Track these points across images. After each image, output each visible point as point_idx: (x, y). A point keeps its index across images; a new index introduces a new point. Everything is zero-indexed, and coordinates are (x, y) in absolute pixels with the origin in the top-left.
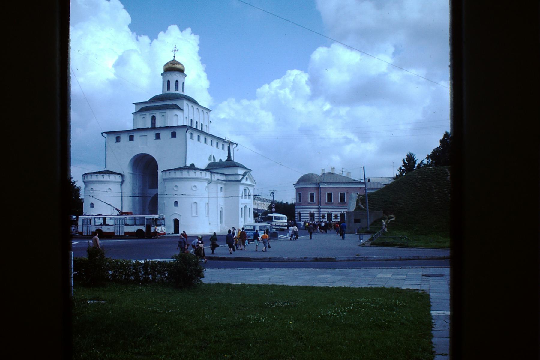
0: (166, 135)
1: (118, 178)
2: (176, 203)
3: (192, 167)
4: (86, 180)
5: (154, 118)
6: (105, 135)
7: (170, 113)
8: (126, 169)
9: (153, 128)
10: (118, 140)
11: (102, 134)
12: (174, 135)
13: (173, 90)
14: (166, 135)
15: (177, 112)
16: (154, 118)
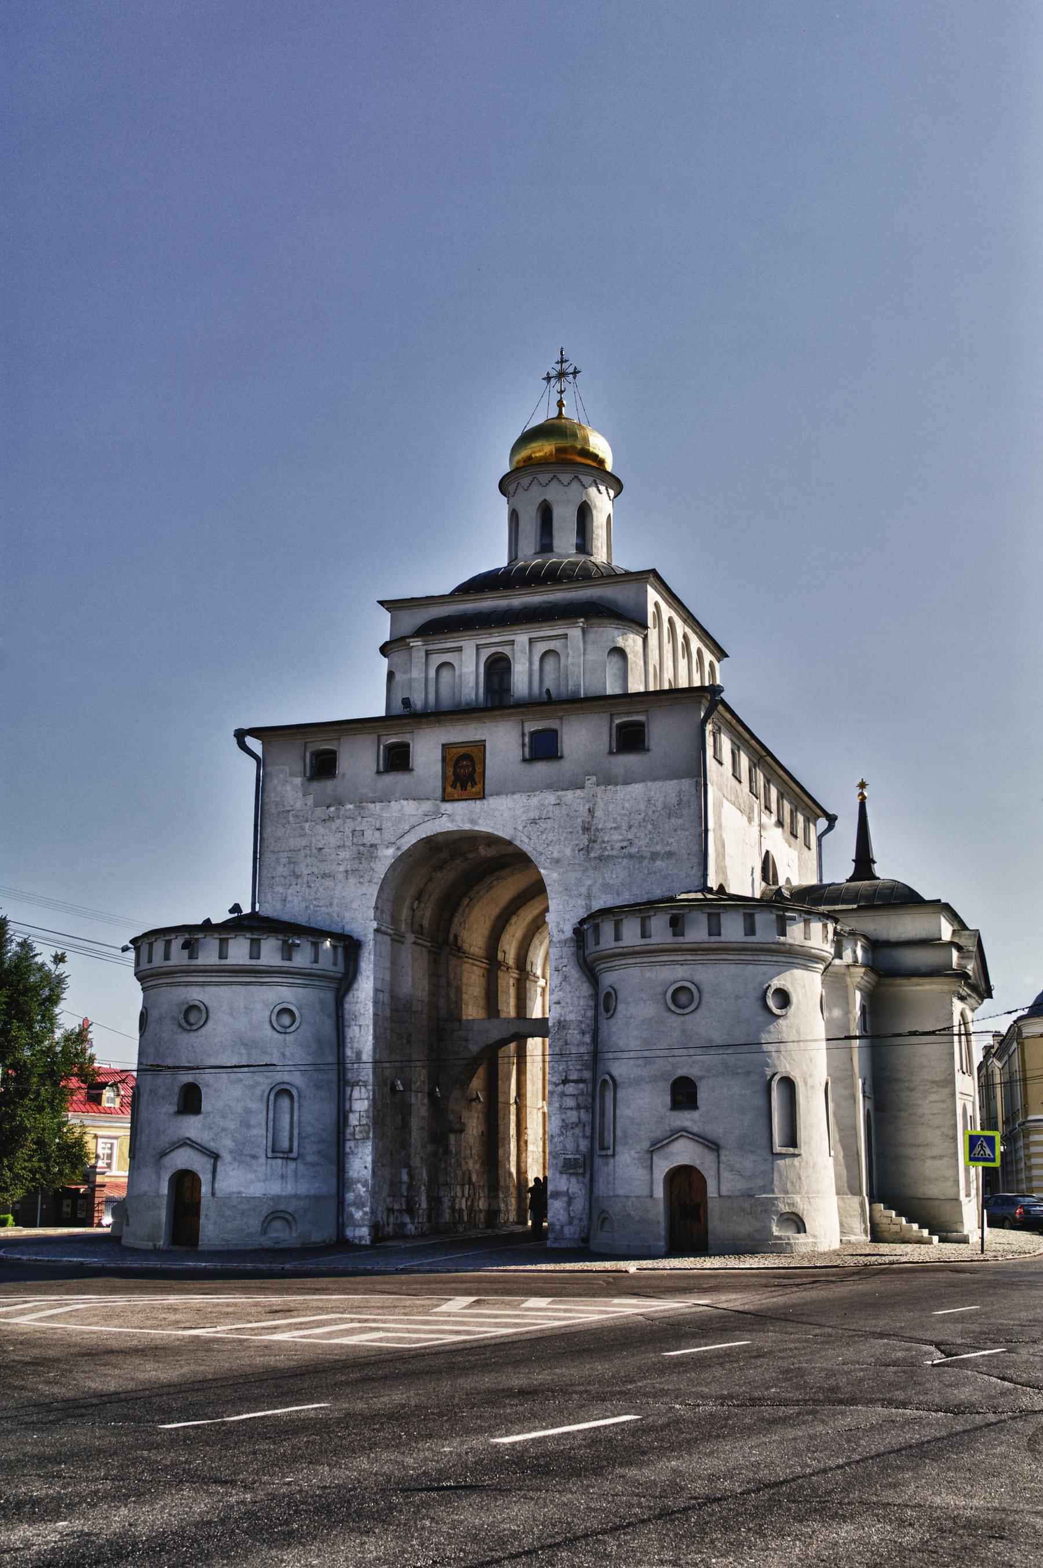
6: (255, 744)
10: (323, 766)
11: (240, 735)
16: (498, 669)
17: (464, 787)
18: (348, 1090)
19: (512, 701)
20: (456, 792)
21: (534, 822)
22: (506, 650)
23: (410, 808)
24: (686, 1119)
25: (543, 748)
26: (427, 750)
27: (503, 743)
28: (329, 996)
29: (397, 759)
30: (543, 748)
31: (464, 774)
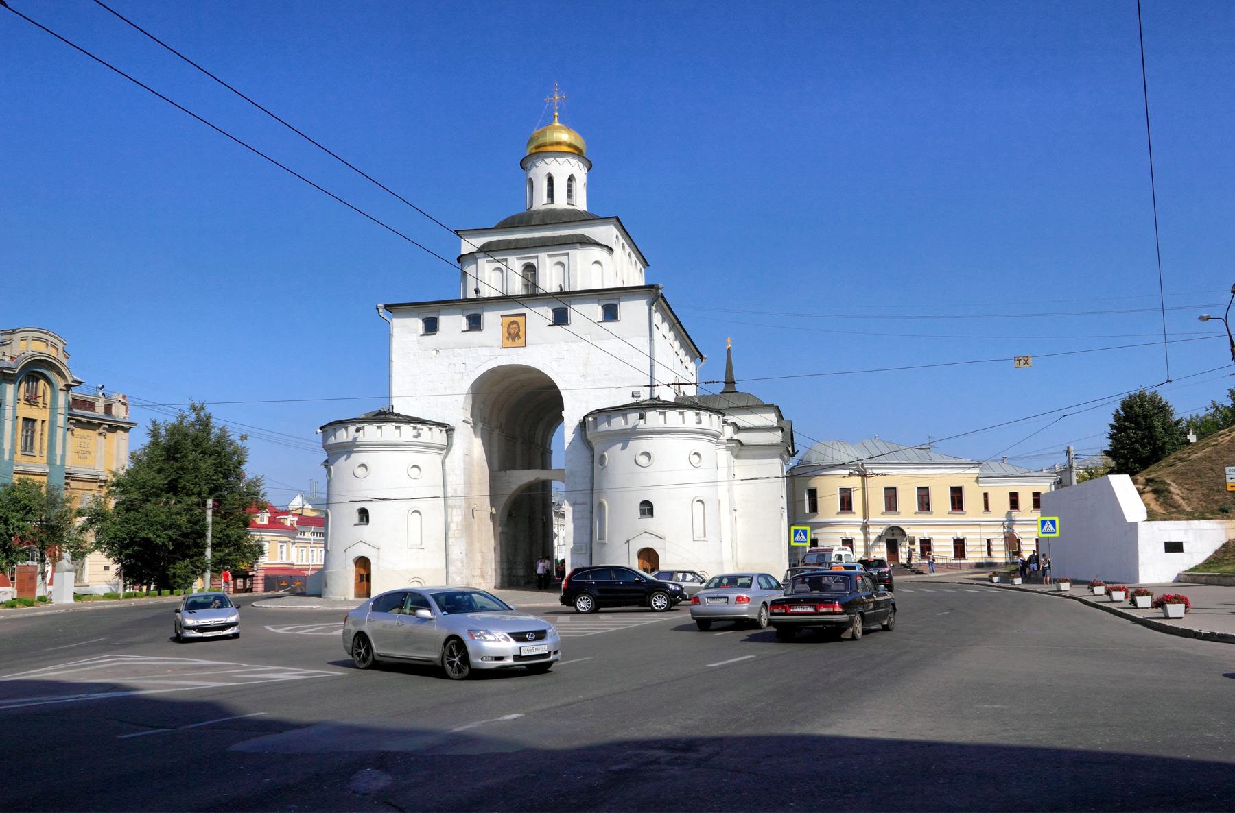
0: (585, 314)
1: (439, 436)
2: (647, 508)
3: (657, 404)
4: (332, 440)
5: (530, 269)
7: (581, 256)
8: (455, 407)
9: (532, 296)
12: (611, 314)
13: (561, 202)
14: (585, 314)
15: (595, 253)
17: (513, 339)
18: (449, 510)
19: (541, 292)
20: (510, 343)
21: (556, 360)
22: (534, 262)
23: (484, 352)
24: (648, 521)
25: (561, 318)
26: (492, 319)
27: (538, 318)
28: (438, 458)
29: (475, 323)
30: (561, 318)
31: (515, 334)
